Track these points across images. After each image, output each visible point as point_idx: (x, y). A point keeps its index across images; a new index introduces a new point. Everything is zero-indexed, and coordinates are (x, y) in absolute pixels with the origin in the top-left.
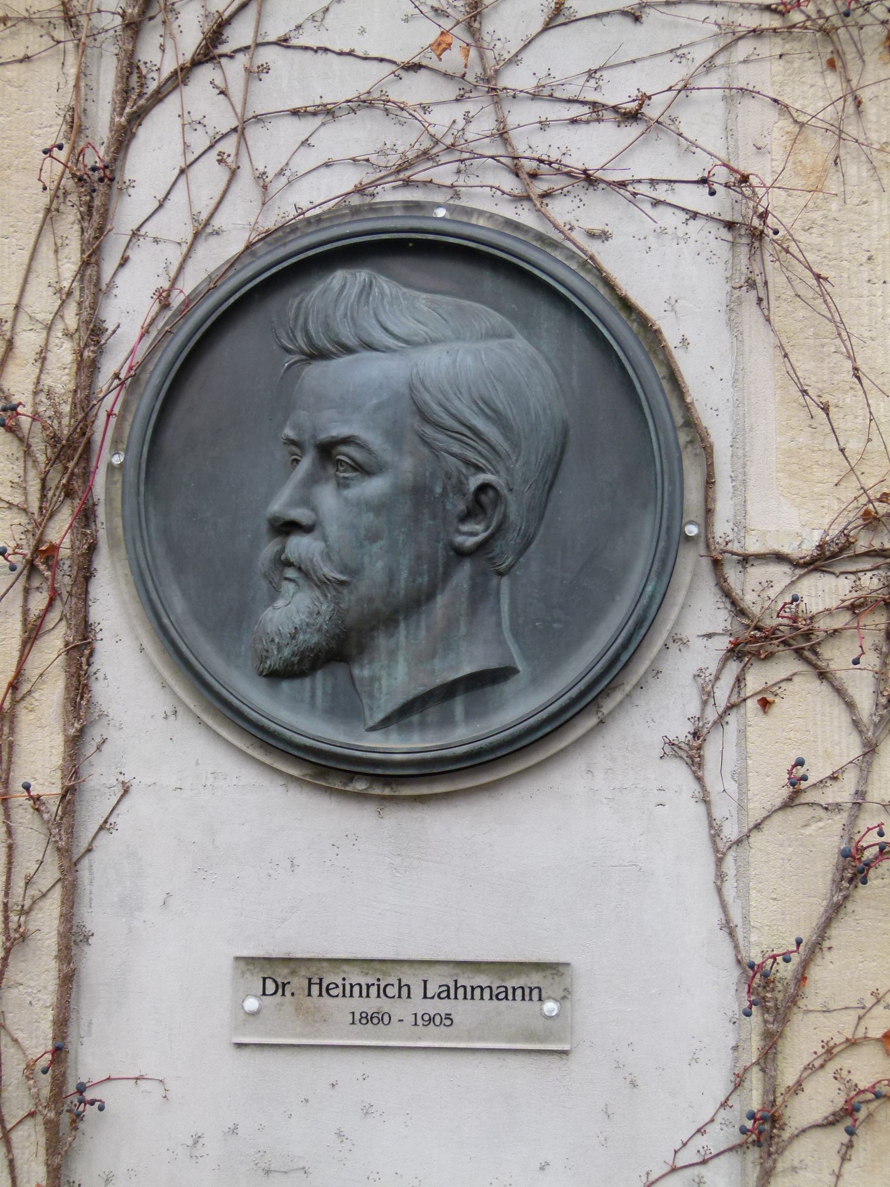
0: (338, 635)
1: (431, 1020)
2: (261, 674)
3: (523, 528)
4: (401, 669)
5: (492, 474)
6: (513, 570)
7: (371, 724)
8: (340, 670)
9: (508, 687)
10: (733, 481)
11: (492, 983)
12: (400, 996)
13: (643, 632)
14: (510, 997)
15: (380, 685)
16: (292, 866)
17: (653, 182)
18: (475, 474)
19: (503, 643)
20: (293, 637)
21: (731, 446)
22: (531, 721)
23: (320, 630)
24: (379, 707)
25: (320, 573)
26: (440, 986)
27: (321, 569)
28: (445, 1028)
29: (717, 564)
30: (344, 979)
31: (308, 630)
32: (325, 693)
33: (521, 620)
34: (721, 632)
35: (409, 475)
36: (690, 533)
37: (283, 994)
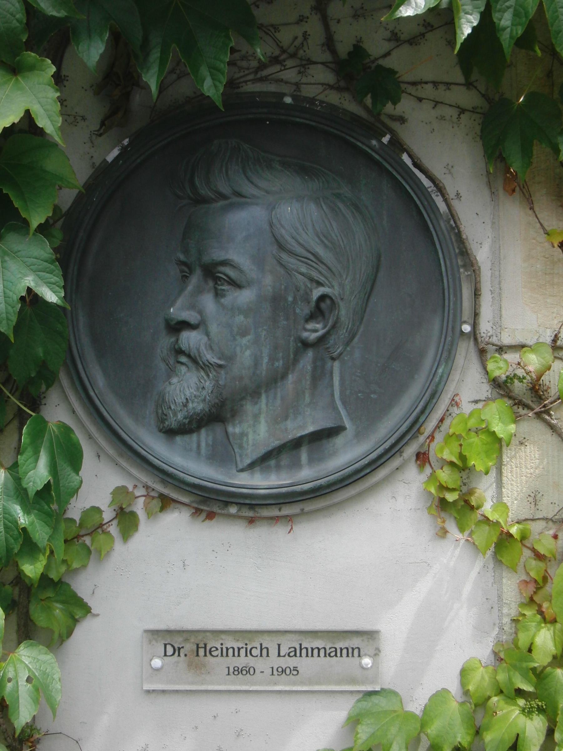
0: (218, 404)
1: (284, 671)
2: (160, 431)
3: (350, 326)
4: (263, 428)
5: (329, 287)
6: (342, 356)
7: (240, 466)
8: (218, 428)
9: (339, 440)
10: (492, 293)
11: (326, 645)
12: (261, 656)
13: (434, 401)
14: (339, 654)
15: (248, 439)
16: (184, 565)
17: (435, 84)
18: (317, 288)
19: (335, 408)
20: (185, 405)
21: (491, 269)
22: (357, 466)
23: (204, 400)
24: (246, 455)
25: (204, 359)
26: (290, 648)
27: (205, 356)
28: (293, 677)
29: (482, 352)
30: (222, 644)
31: (196, 400)
32: (207, 444)
33: (348, 392)
34: (484, 399)
35: (269, 288)
36: (465, 330)
37: (179, 655)
